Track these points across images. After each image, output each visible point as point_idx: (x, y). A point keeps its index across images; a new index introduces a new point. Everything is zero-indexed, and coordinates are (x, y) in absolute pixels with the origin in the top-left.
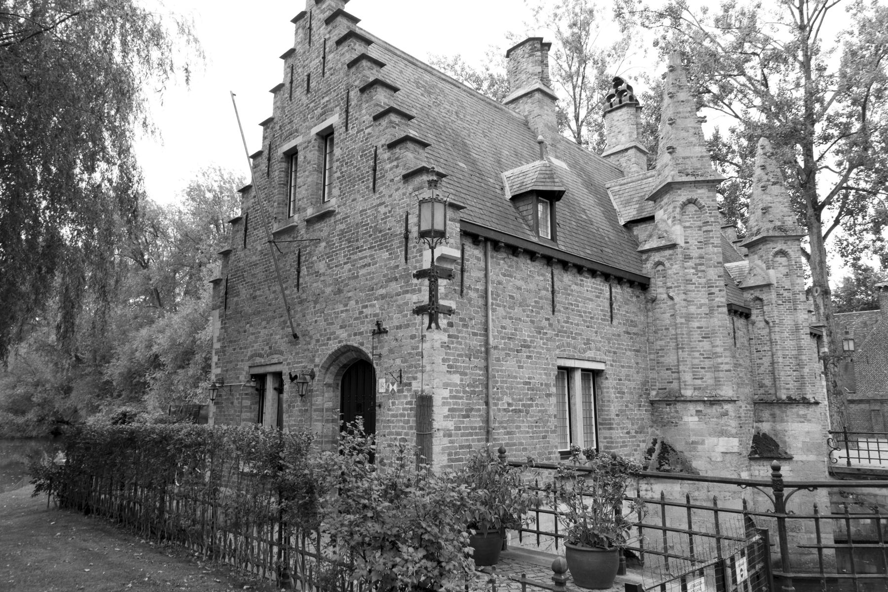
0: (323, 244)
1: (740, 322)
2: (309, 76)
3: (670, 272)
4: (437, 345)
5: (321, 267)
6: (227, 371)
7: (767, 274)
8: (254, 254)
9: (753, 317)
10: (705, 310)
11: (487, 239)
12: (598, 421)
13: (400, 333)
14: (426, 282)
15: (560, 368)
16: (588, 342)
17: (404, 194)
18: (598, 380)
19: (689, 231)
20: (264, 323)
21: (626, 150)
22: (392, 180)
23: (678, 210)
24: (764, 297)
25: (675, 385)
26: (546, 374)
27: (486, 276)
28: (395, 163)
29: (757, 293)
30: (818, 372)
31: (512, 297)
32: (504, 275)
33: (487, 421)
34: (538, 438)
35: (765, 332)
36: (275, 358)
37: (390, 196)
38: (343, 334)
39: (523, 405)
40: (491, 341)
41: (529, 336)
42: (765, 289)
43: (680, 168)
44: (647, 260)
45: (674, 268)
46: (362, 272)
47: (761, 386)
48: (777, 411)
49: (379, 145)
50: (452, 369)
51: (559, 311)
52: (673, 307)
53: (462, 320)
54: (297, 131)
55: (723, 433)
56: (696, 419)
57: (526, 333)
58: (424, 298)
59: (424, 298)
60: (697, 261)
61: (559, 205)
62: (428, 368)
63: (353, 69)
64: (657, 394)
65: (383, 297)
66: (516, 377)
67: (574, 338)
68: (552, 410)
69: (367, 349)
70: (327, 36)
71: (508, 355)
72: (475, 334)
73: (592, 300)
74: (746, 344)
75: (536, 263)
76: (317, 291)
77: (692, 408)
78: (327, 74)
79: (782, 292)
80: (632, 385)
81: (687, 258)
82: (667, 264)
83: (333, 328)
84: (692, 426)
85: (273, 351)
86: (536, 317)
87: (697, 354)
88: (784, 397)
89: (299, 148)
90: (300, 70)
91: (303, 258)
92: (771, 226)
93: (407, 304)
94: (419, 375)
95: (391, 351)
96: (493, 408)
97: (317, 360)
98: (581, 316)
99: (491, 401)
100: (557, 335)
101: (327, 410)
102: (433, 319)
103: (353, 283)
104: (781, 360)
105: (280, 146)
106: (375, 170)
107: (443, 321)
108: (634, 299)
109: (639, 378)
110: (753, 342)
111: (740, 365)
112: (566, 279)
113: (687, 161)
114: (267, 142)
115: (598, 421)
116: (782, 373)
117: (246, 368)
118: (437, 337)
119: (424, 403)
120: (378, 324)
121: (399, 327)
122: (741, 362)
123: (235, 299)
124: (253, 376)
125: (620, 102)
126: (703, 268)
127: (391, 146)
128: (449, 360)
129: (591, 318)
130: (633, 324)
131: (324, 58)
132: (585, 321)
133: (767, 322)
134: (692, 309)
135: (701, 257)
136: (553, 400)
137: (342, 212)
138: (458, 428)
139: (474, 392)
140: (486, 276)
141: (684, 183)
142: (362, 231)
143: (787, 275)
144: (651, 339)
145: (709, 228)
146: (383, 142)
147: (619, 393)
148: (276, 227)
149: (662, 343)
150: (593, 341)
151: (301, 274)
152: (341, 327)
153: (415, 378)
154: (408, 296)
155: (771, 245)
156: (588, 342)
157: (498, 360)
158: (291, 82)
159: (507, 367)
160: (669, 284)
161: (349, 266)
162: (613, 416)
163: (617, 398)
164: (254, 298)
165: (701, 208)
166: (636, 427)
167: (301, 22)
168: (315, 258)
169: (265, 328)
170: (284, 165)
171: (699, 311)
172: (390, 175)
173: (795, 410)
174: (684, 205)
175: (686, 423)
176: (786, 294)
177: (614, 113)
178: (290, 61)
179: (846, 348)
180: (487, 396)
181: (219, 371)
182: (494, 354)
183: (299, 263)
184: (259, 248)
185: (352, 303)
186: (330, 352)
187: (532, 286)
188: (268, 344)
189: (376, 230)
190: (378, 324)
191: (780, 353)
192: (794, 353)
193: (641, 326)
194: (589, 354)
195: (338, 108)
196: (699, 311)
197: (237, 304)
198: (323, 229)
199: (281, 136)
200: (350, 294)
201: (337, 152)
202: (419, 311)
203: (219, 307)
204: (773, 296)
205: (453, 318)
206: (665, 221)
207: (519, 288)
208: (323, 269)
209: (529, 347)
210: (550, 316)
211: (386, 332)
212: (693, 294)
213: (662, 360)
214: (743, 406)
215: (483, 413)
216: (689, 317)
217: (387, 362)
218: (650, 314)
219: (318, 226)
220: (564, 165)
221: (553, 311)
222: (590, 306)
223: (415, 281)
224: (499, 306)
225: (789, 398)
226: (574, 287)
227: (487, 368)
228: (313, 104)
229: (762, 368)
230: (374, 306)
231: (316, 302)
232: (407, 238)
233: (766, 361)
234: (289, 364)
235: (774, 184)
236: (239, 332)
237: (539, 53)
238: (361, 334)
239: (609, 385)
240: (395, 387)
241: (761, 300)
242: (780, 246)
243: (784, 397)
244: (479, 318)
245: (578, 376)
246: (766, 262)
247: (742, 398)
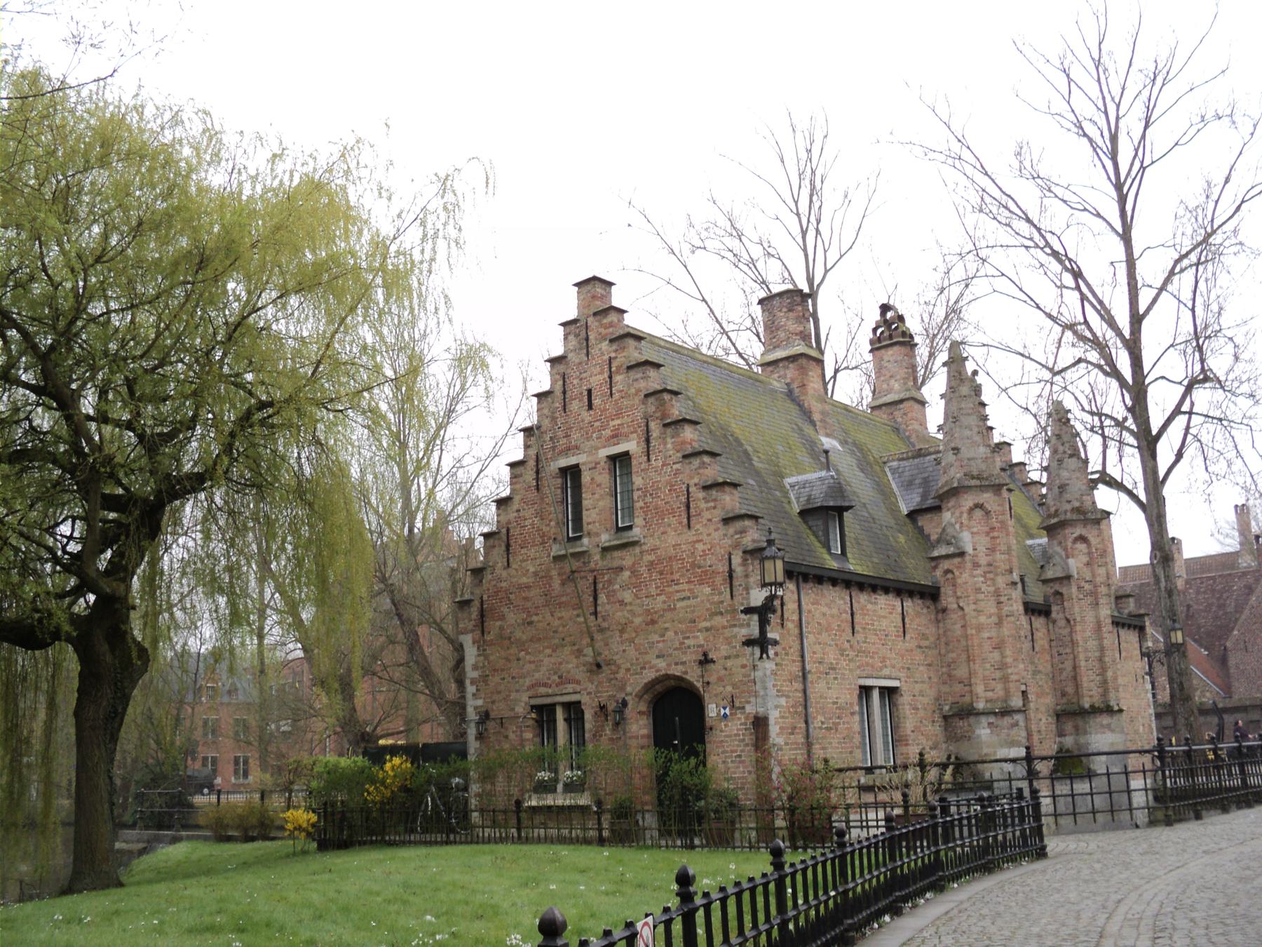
0: (627, 574)
1: (1039, 622)
2: (589, 391)
3: (959, 581)
4: (768, 673)
5: (627, 596)
6: (493, 702)
7: (1067, 564)
8: (525, 575)
9: (1054, 615)
10: (994, 619)
11: (799, 573)
12: (896, 738)
13: (729, 663)
14: (756, 617)
15: (861, 687)
16: (883, 660)
17: (725, 535)
18: (895, 697)
19: (977, 537)
20: (548, 651)
21: (901, 401)
22: (710, 520)
23: (965, 515)
24: (1064, 590)
25: (967, 699)
27: (800, 606)
28: (712, 504)
29: (1057, 587)
30: (1140, 673)
31: (819, 624)
32: (813, 604)
33: (807, 736)
35: (1066, 631)
36: (570, 688)
37: (709, 535)
38: (662, 664)
40: (808, 667)
42: (1065, 582)
43: (965, 470)
44: (935, 567)
45: (964, 577)
46: (679, 605)
47: (1064, 694)
48: (1080, 722)
49: (692, 482)
50: (781, 693)
52: (964, 617)
54: (577, 447)
55: (1013, 744)
56: (988, 731)
57: (832, 657)
58: (755, 631)
59: (755, 631)
60: (986, 569)
61: (847, 515)
62: (762, 693)
63: (651, 400)
64: (951, 708)
65: (707, 629)
67: (872, 657)
68: (857, 727)
69: (693, 676)
70: (613, 355)
72: (794, 661)
73: (885, 617)
74: (1047, 647)
75: (837, 588)
76: (623, 621)
77: (984, 720)
78: (617, 396)
79: (1083, 584)
80: (926, 700)
81: (976, 565)
82: (957, 573)
83: (647, 658)
84: (984, 738)
85: (563, 680)
87: (988, 666)
88: (1087, 706)
89: (583, 468)
90: (575, 382)
91: (600, 586)
92: (1068, 507)
93: (735, 636)
94: (752, 699)
95: (720, 679)
96: (811, 726)
97: (629, 689)
99: (810, 721)
101: (643, 737)
102: (764, 651)
103: (668, 615)
104: (1083, 663)
105: (553, 459)
106: (688, 507)
107: (771, 652)
108: (925, 611)
109: (932, 693)
110: (1053, 644)
111: (1039, 672)
112: (862, 599)
113: (972, 463)
114: (532, 452)
115: (896, 738)
116: (1085, 679)
117: (525, 698)
118: (769, 666)
119: (760, 723)
120: (705, 655)
121: (726, 658)
122: (1040, 668)
123: (498, 623)
124: (533, 707)
125: (891, 337)
126: (991, 576)
127: (706, 488)
130: (925, 637)
131: (610, 377)
133: (1068, 621)
134: (982, 619)
135: (990, 565)
136: (857, 718)
137: (650, 543)
138: (786, 744)
140: (800, 606)
141: (970, 487)
142: (676, 566)
143: (1088, 564)
144: (943, 651)
145: (996, 534)
146: (696, 480)
148: (556, 550)
149: (954, 655)
151: (599, 602)
152: (658, 657)
153: (749, 702)
154: (736, 630)
155: (1068, 531)
156: (883, 660)
158: (564, 392)
159: (818, 688)
160: (959, 594)
161: (663, 597)
162: (909, 732)
164: (530, 623)
165: (988, 513)
166: (930, 743)
167: (573, 327)
168: (617, 587)
169: (550, 656)
170: (559, 481)
171: (990, 621)
172: (707, 515)
173: (1098, 720)
174: (971, 510)
175: (979, 736)
176: (1087, 586)
177: (883, 351)
178: (561, 368)
179: (1173, 640)
180: (806, 715)
181: (480, 702)
182: (809, 676)
183: (595, 590)
184: (532, 569)
185: (670, 634)
186: (646, 681)
187: (835, 611)
188: (555, 673)
189: (693, 565)
190: (705, 655)
191: (1082, 656)
192: (1097, 654)
193: (932, 639)
194: (886, 672)
195: (635, 435)
196: (990, 621)
197: (501, 628)
198: (626, 558)
199: (554, 448)
200: (667, 625)
201: (638, 481)
202: (749, 643)
203: (472, 631)
204: (1074, 589)
205: (778, 648)
206: (953, 525)
207: (824, 615)
208: (625, 600)
209: (834, 669)
210: (850, 637)
211: (713, 661)
212: (982, 604)
213: (954, 672)
214: (1044, 720)
215: (804, 730)
216: (980, 628)
217: (716, 688)
218: (941, 625)
219: (617, 554)
220: (836, 444)
222: (884, 623)
223: (743, 616)
225: (1092, 706)
226: (869, 606)
227: (805, 691)
228: (598, 424)
229: (1064, 674)
230: (697, 637)
231: (622, 631)
232: (731, 577)
233: (1068, 665)
234: (589, 693)
235: (1071, 456)
236: (508, 660)
237: (800, 308)
238: (683, 663)
239: (904, 700)
240: (727, 711)
241: (1061, 594)
242: (1078, 531)
243: (1087, 706)
244: (796, 646)
245: (876, 695)
246: (1065, 549)
247: (1043, 709)
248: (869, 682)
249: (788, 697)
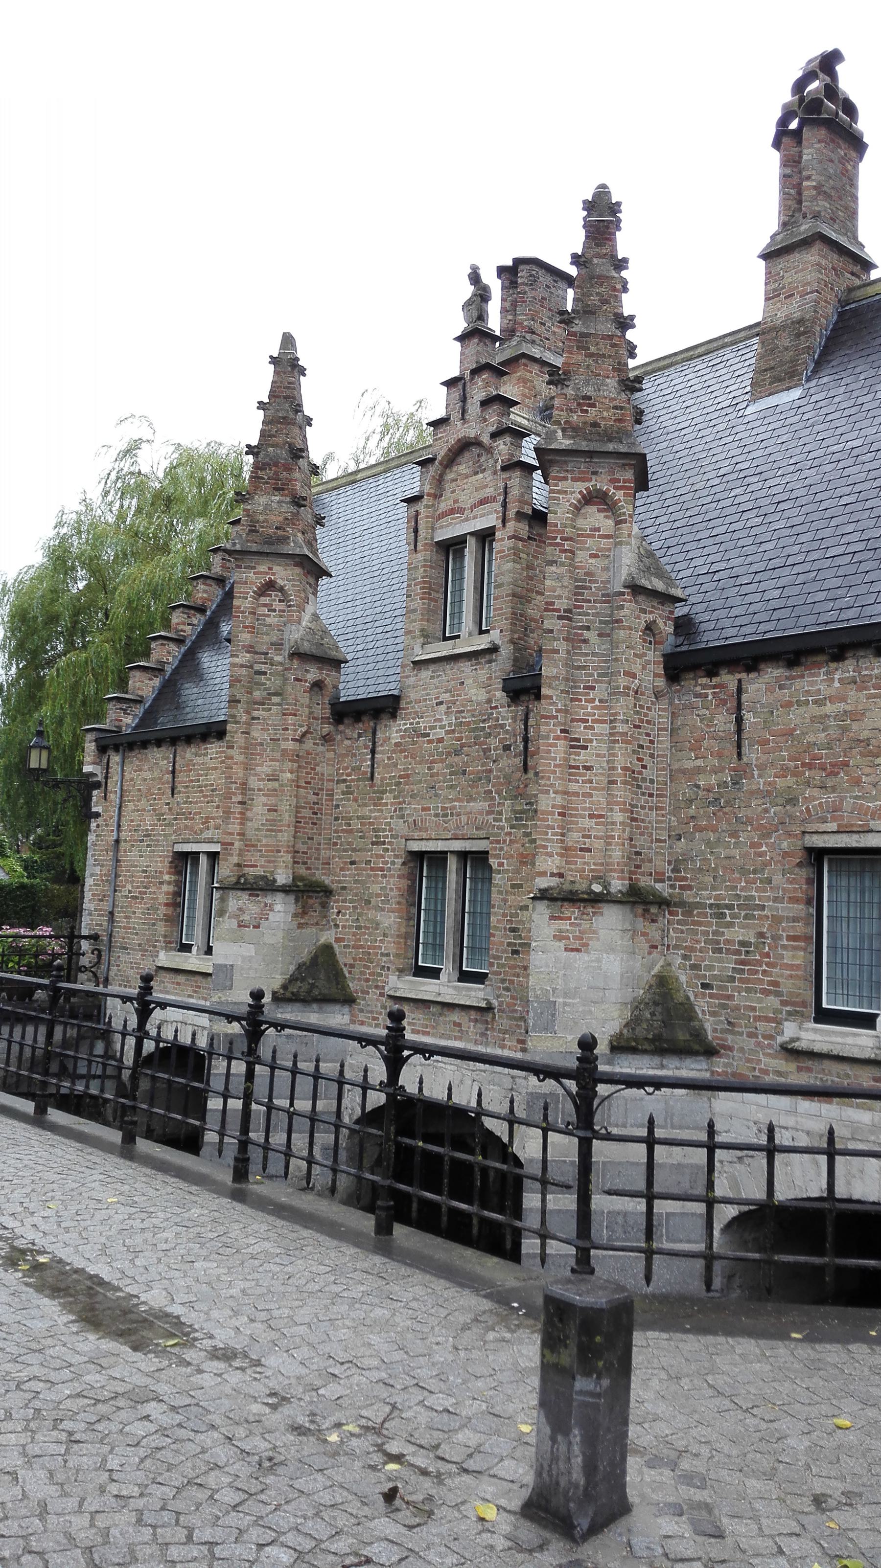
16: (206, 821)
34: (148, 924)
39: (140, 892)
51: (179, 792)
53: (105, 820)
57: (149, 821)
66: (136, 866)
71: (133, 846)
73: (215, 769)
98: (201, 791)
100: (176, 819)
129: (213, 791)
132: (205, 796)
138: (96, 910)
150: (212, 818)
194: (208, 834)
205: (100, 820)
209: (149, 835)
221: (173, 794)
226: (199, 760)
248: (194, 848)
249: (102, 866)
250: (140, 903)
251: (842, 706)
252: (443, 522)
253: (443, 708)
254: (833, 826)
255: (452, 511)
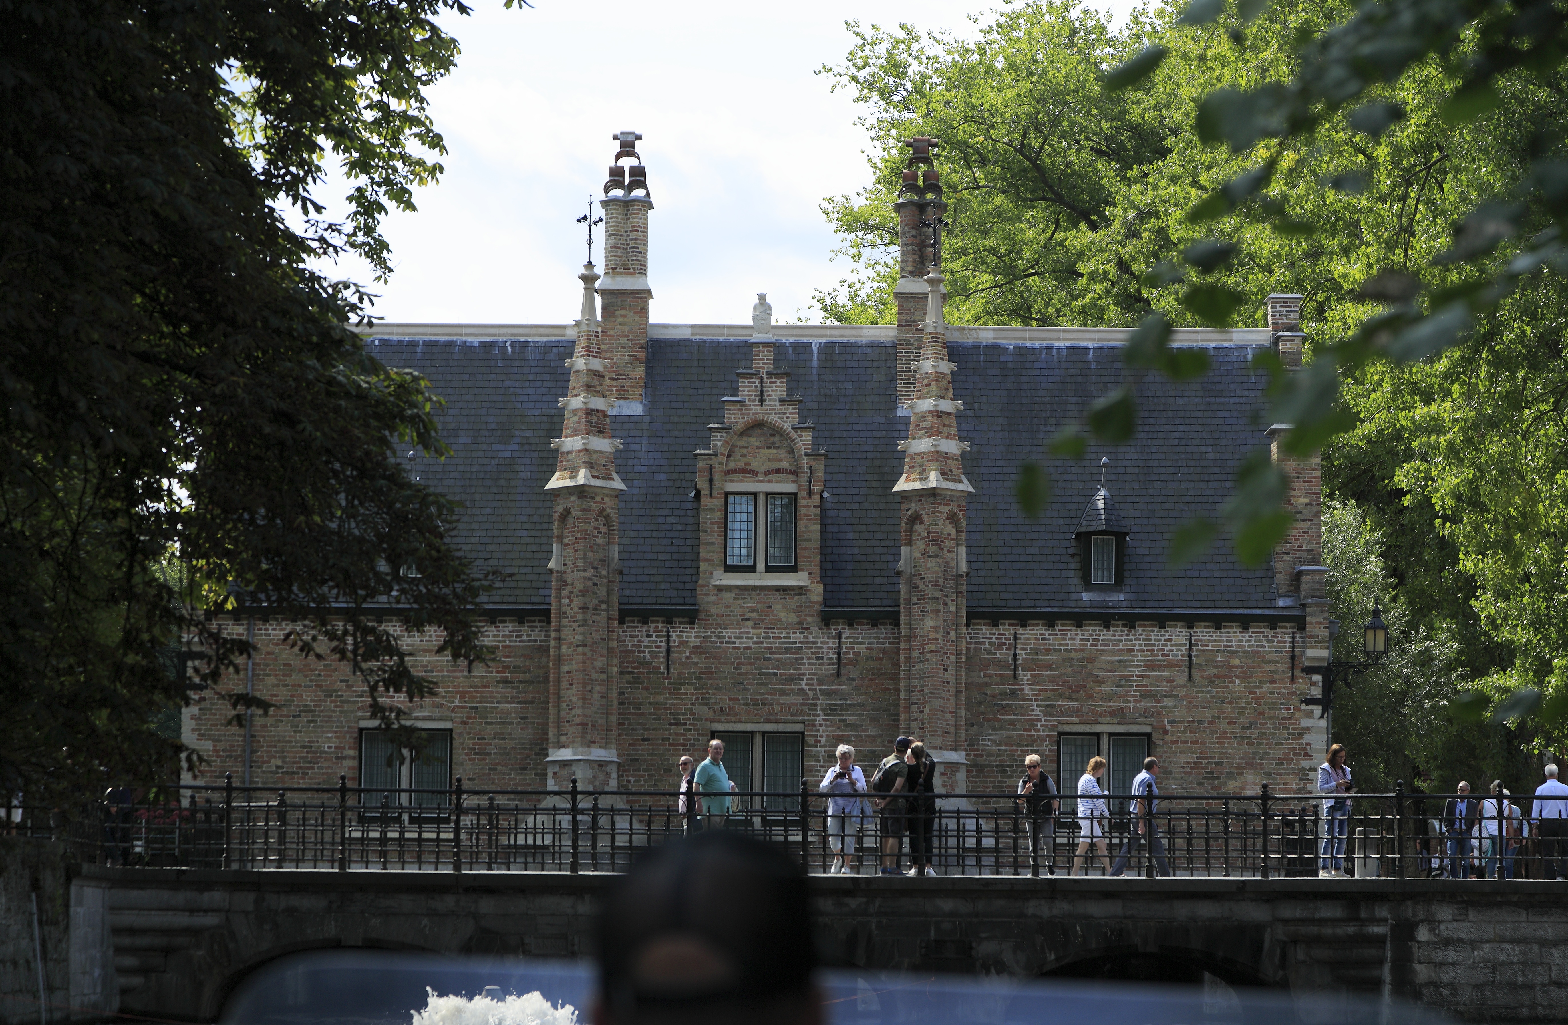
26: (337, 737)
39: (300, 768)
41: (311, 701)
66: (290, 742)
80: (509, 744)
86: (325, 681)
128: (200, 730)
139: (231, 757)
147: (476, 754)
157: (265, 726)
163: (470, 760)
209: (312, 711)
224: (267, 675)
250: (303, 778)
251: (1081, 654)
252: (735, 477)
253: (750, 624)
254: (1077, 720)
255: (743, 471)
